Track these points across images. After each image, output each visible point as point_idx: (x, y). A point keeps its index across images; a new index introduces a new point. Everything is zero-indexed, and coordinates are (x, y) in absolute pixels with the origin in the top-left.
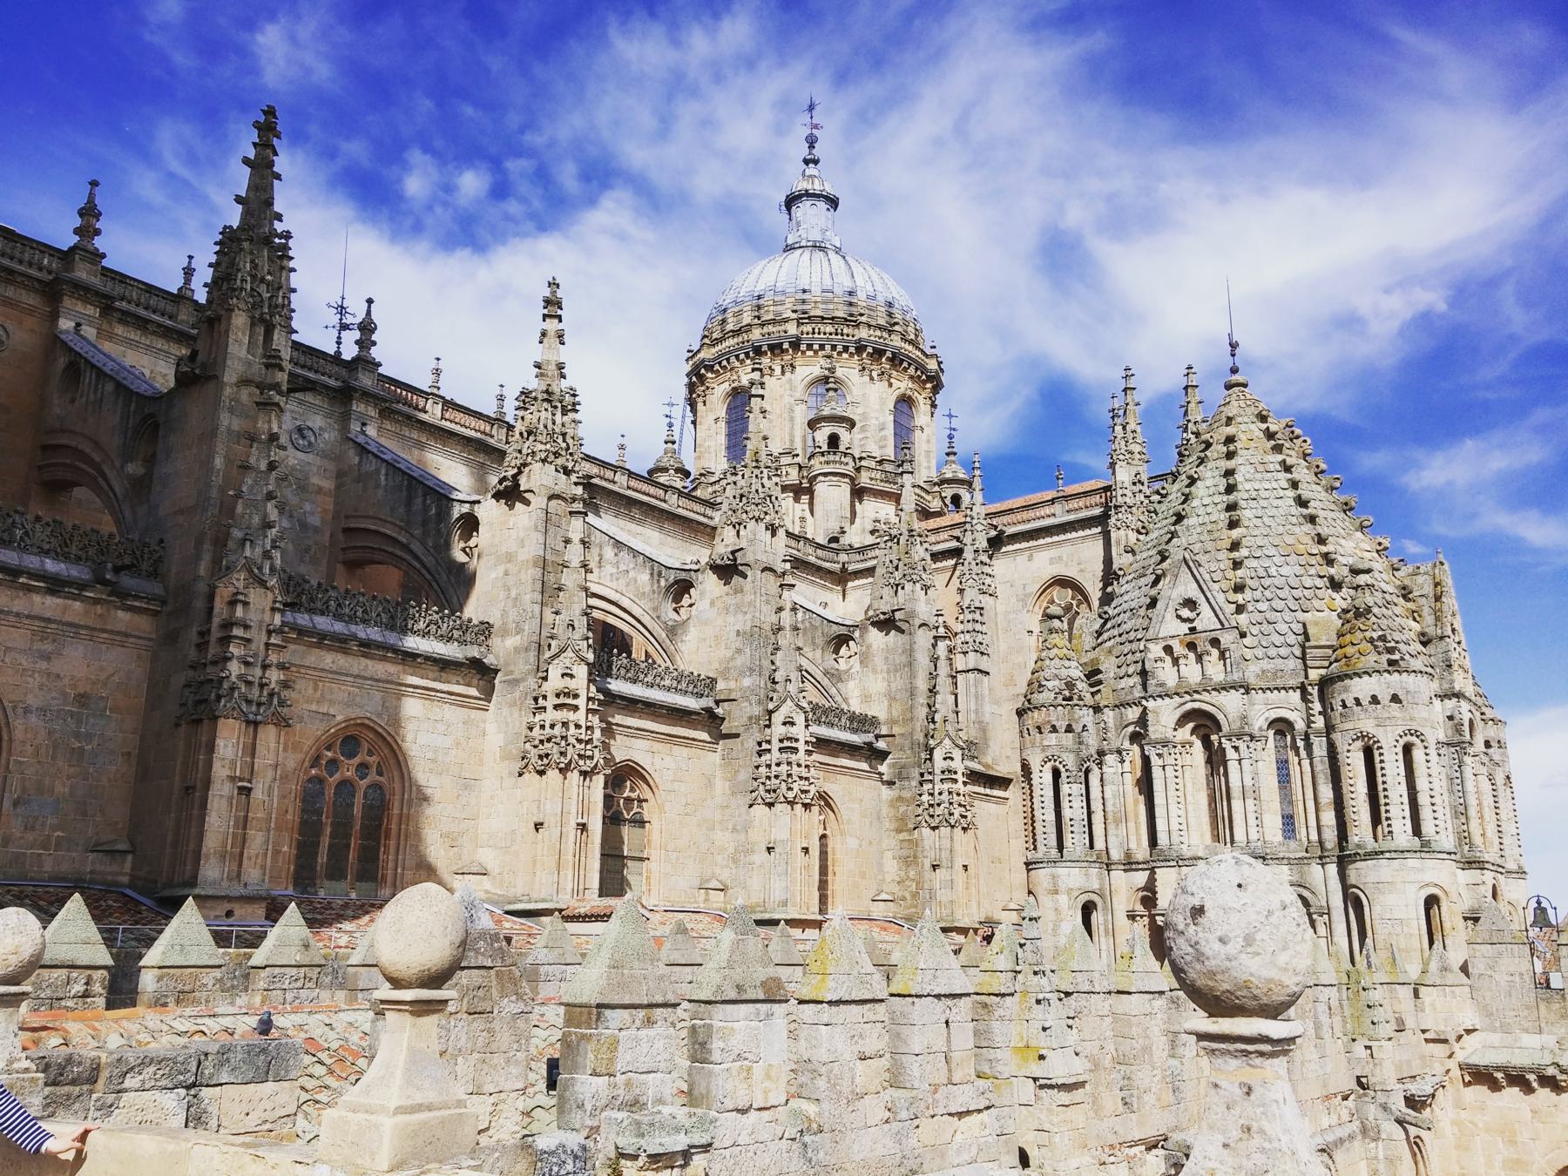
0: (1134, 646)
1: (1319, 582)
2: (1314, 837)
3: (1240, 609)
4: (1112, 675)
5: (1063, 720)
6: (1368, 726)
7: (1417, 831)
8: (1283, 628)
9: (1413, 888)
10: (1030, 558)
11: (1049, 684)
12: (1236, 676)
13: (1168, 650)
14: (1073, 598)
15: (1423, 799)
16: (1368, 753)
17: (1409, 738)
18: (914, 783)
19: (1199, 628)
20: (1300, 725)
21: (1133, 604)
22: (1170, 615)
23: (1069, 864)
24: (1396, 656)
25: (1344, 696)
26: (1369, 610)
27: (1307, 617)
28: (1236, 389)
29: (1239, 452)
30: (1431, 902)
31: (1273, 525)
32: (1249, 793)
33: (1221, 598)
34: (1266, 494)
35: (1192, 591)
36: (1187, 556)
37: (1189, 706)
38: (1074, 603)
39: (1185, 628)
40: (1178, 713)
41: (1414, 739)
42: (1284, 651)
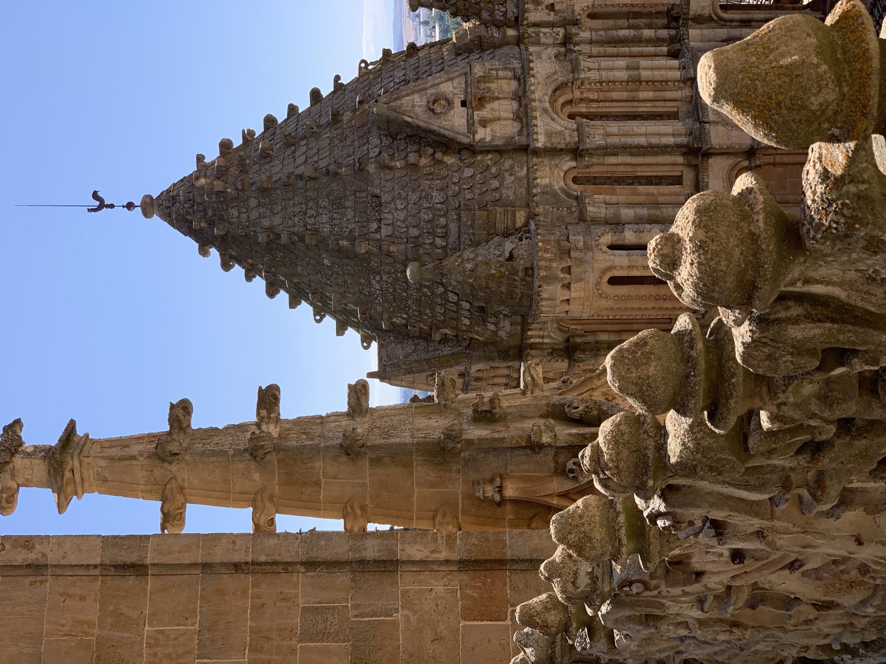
2: (665, 49)
21: (414, 197)
37: (547, 105)
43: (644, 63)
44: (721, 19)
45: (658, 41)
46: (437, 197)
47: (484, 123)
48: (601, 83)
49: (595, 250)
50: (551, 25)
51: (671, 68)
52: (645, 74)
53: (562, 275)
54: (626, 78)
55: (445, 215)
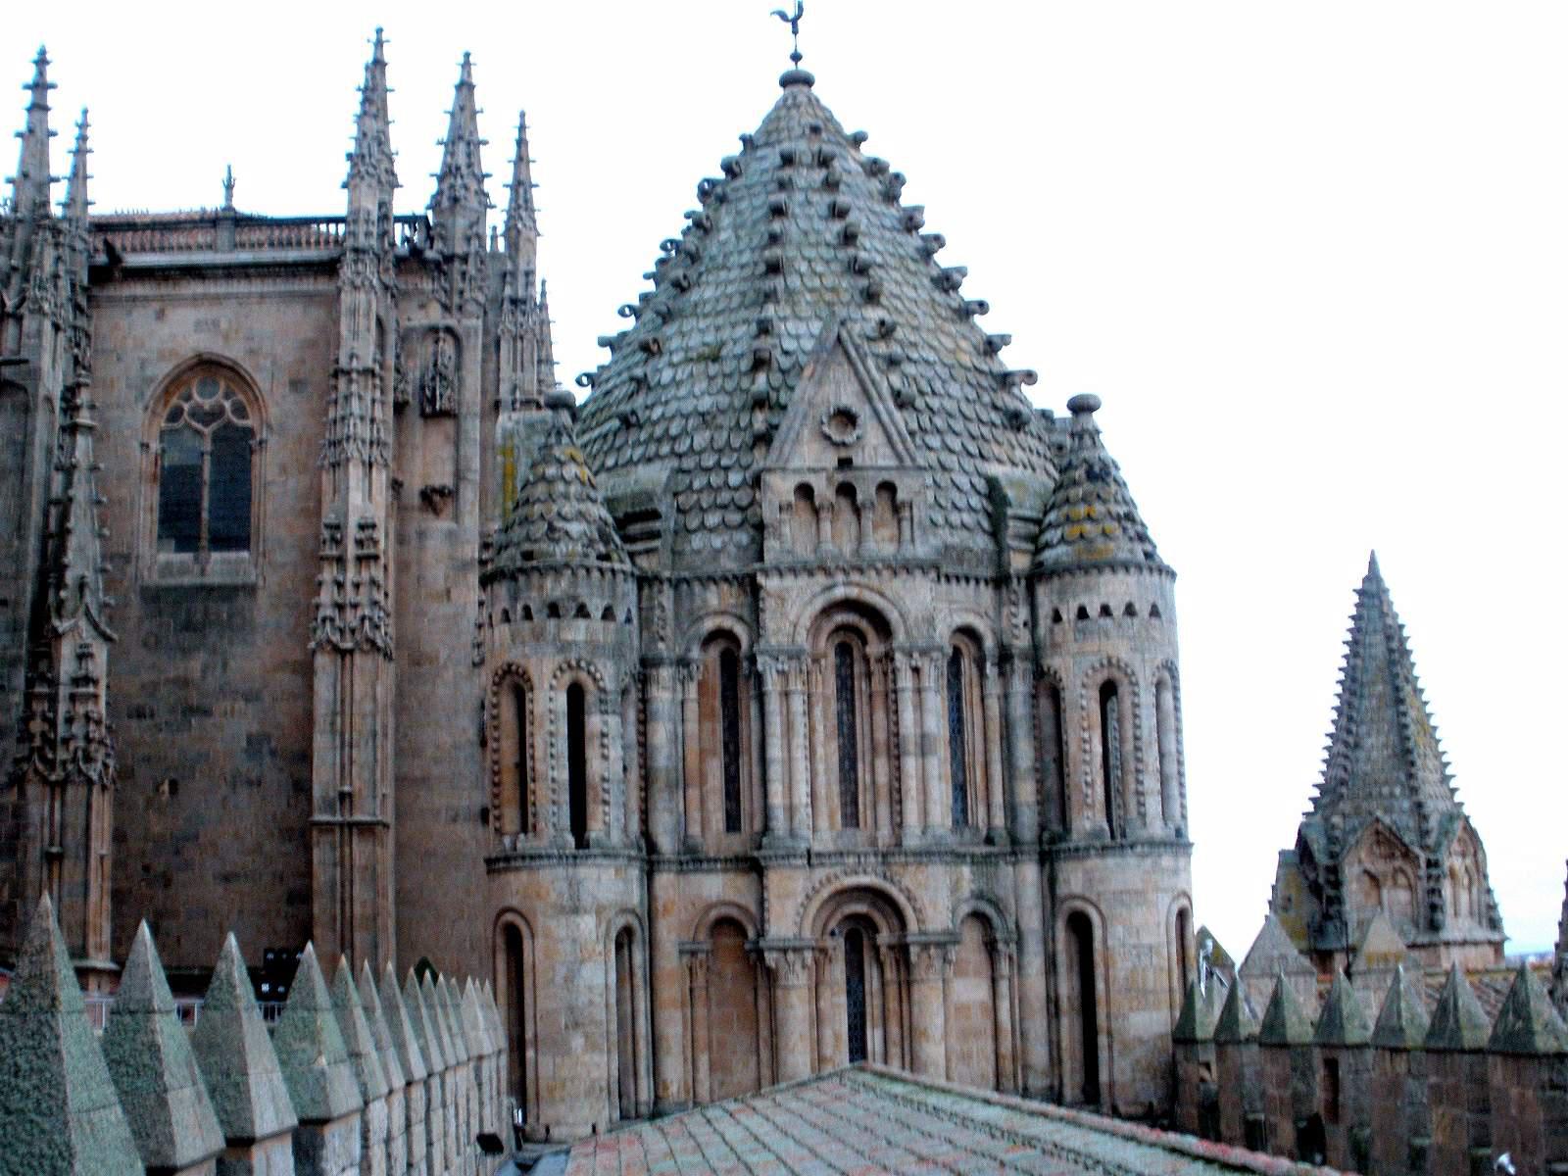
0: (716, 479)
1: (996, 417)
2: (999, 820)
4: (672, 524)
5: (602, 596)
6: (1121, 650)
8: (963, 481)
10: (160, 315)
11: (575, 528)
14: (227, 396)
18: (17, 698)
19: (857, 461)
21: (706, 403)
23: (599, 861)
25: (1084, 600)
27: (994, 469)
29: (842, 187)
31: (919, 313)
36: (844, 335)
37: (840, 592)
38: (227, 405)
39: (831, 459)
40: (819, 603)
41: (1167, 675)
42: (967, 518)
43: (939, 765)
44: (1054, 915)
45: (1011, 809)
46: (701, 440)
47: (805, 491)
48: (895, 692)
49: (560, 659)
50: (1033, 624)
51: (925, 813)
52: (910, 764)
53: (519, 607)
54: (902, 731)
55: (673, 453)
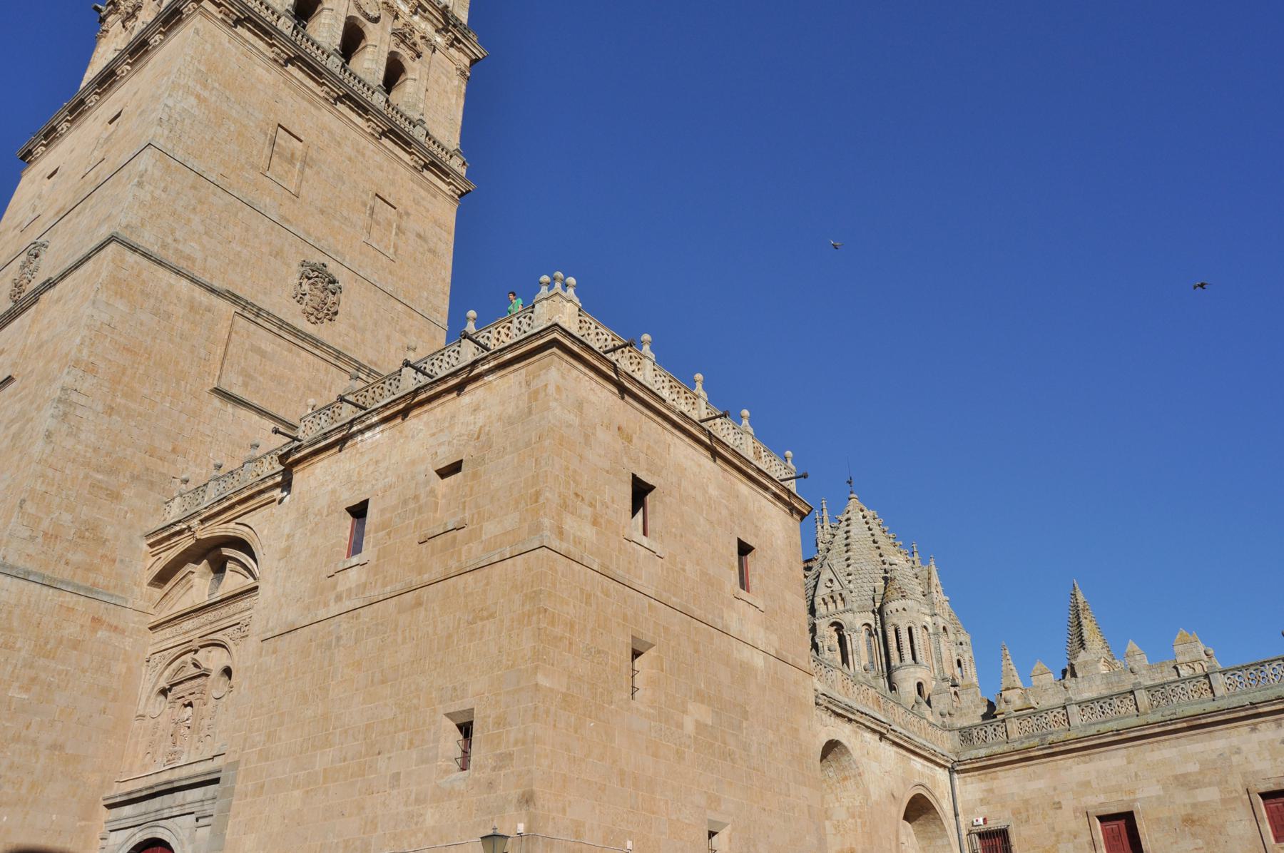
3: (850, 582)
6: (895, 621)
7: (914, 658)
8: (867, 589)
9: (912, 680)
12: (848, 607)
13: (823, 599)
15: (916, 647)
16: (896, 631)
17: (912, 625)
19: (834, 590)
20: (873, 626)
22: (823, 586)
24: (905, 594)
26: (895, 579)
28: (852, 500)
30: (919, 685)
32: (855, 652)
33: (843, 579)
34: (861, 539)
35: (832, 576)
37: (832, 621)
39: (829, 590)
